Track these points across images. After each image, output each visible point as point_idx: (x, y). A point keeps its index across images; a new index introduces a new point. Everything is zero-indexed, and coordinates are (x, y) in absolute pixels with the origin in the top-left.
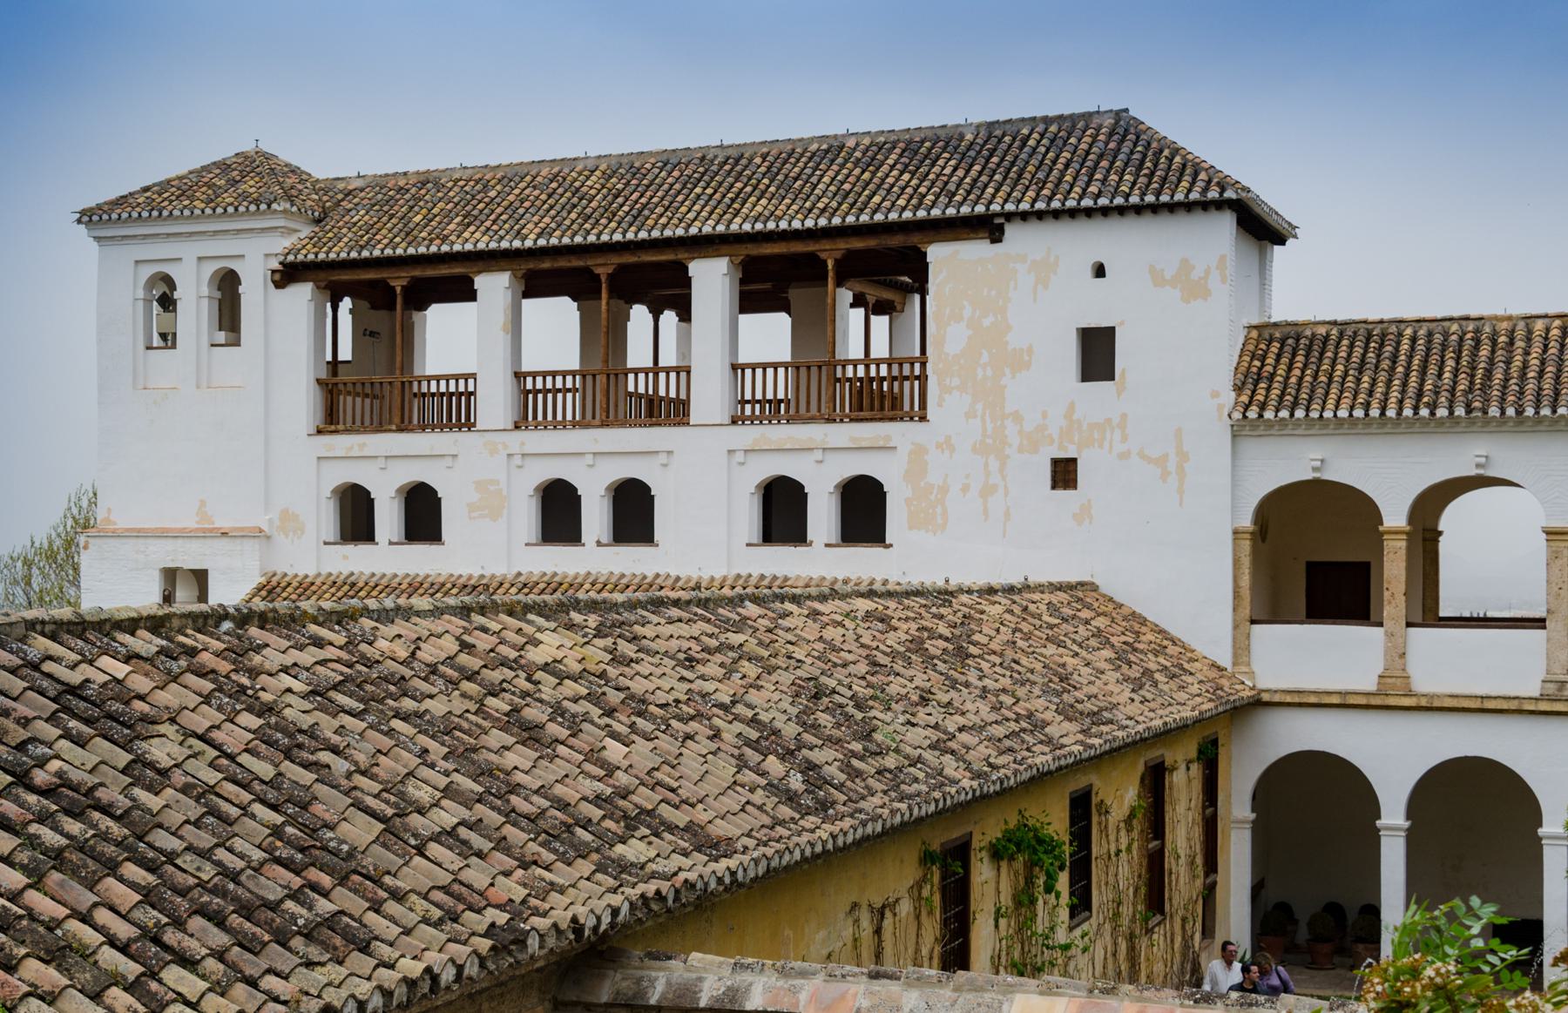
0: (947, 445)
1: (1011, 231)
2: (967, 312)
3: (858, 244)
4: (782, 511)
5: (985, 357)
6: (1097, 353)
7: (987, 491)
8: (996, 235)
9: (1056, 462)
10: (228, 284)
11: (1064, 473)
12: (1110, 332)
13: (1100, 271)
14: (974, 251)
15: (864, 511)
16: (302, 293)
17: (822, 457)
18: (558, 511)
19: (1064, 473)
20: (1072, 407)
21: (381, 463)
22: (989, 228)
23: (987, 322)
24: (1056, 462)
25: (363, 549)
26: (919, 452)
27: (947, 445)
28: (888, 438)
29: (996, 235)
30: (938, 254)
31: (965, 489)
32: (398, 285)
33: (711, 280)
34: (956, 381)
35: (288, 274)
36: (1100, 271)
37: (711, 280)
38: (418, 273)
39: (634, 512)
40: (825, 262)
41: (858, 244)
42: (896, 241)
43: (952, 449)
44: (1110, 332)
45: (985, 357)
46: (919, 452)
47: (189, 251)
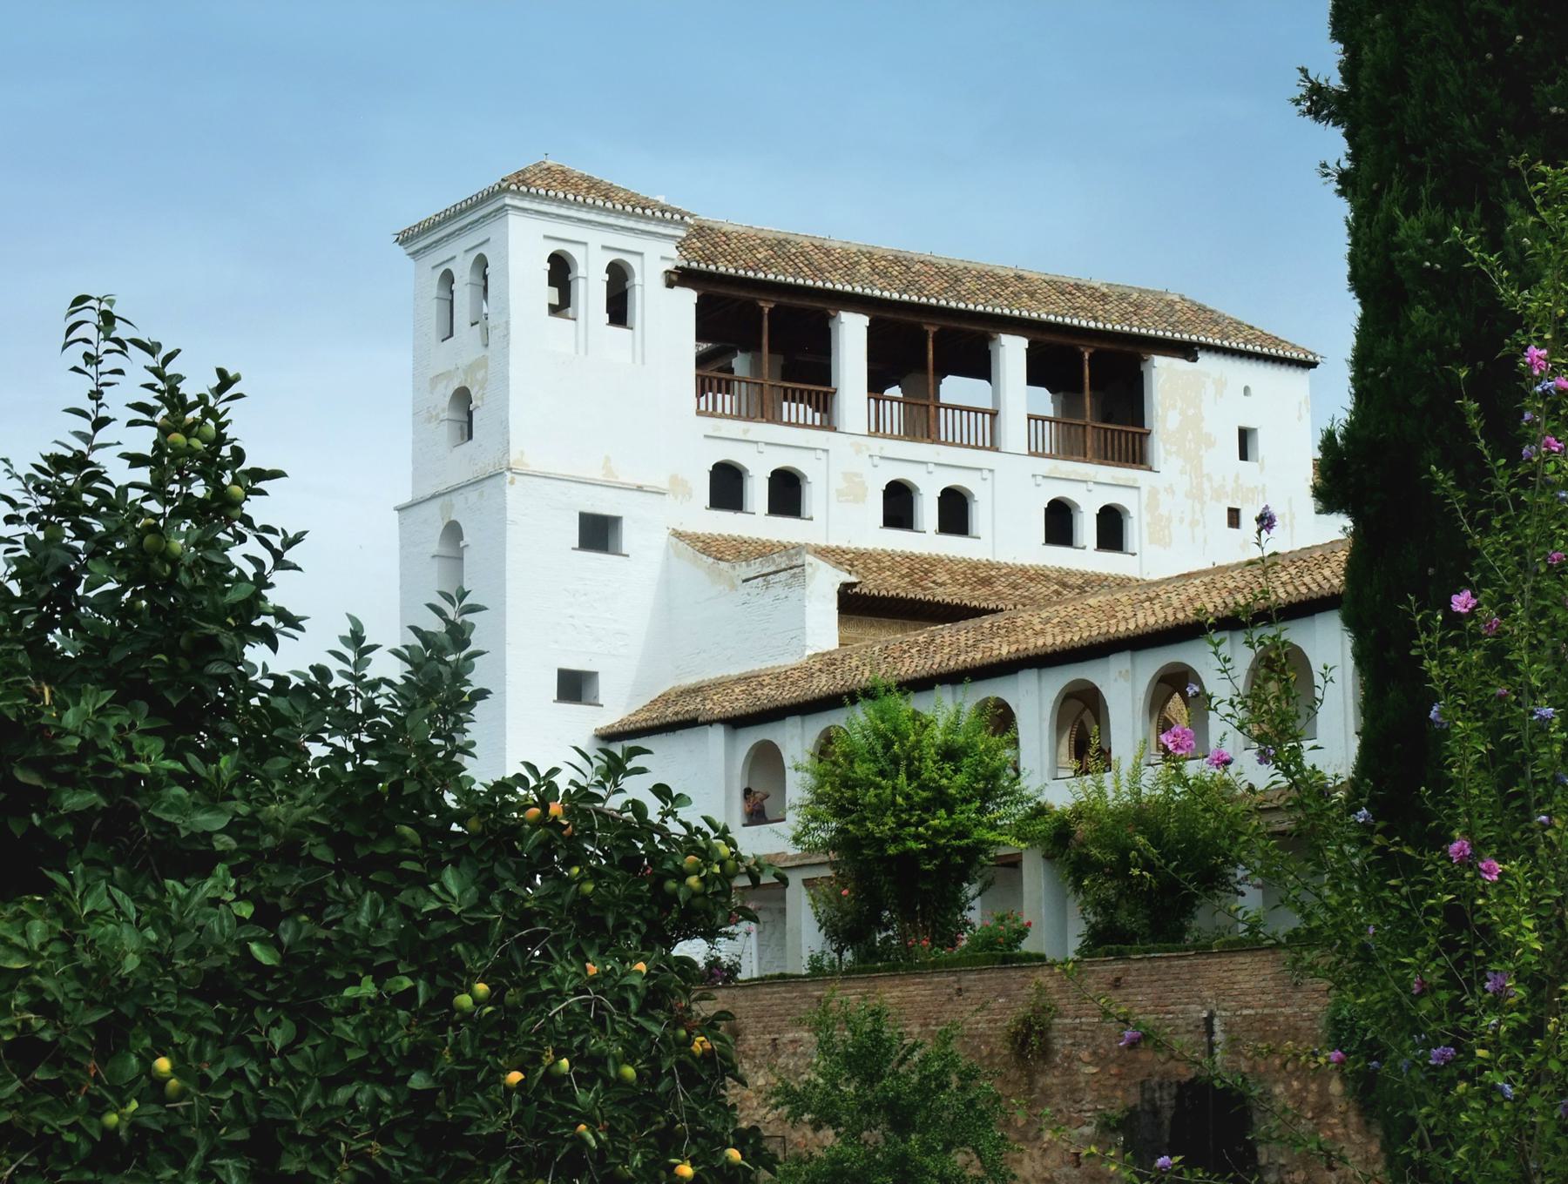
0: (1170, 490)
1: (1205, 359)
2: (1179, 404)
3: (1106, 346)
5: (1190, 436)
7: (1194, 524)
9: (1230, 510)
10: (618, 278)
13: (1247, 391)
15: (1112, 529)
16: (687, 298)
17: (1091, 486)
18: (898, 505)
20: (1237, 477)
21: (762, 447)
23: (1191, 412)
24: (1230, 510)
26: (1154, 493)
27: (1170, 490)
28: (1135, 480)
31: (1182, 520)
32: (766, 307)
33: (1012, 352)
34: (1174, 449)
36: (1247, 391)
37: (1012, 352)
38: (784, 300)
39: (955, 511)
40: (1082, 354)
41: (1106, 346)
43: (1173, 492)
45: (1190, 436)
46: (1154, 493)
47: (596, 238)
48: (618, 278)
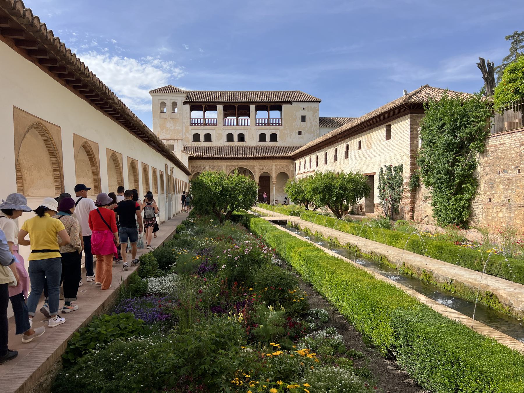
4: (263, 137)
6: (303, 119)
8: (291, 104)
11: (300, 133)
12: (305, 116)
14: (289, 105)
15: (274, 137)
19: (300, 133)
22: (290, 103)
25: (199, 143)
29: (291, 104)
30: (284, 106)
33: (252, 107)
35: (185, 103)
42: (278, 104)
44: (305, 116)
48: (174, 105)
